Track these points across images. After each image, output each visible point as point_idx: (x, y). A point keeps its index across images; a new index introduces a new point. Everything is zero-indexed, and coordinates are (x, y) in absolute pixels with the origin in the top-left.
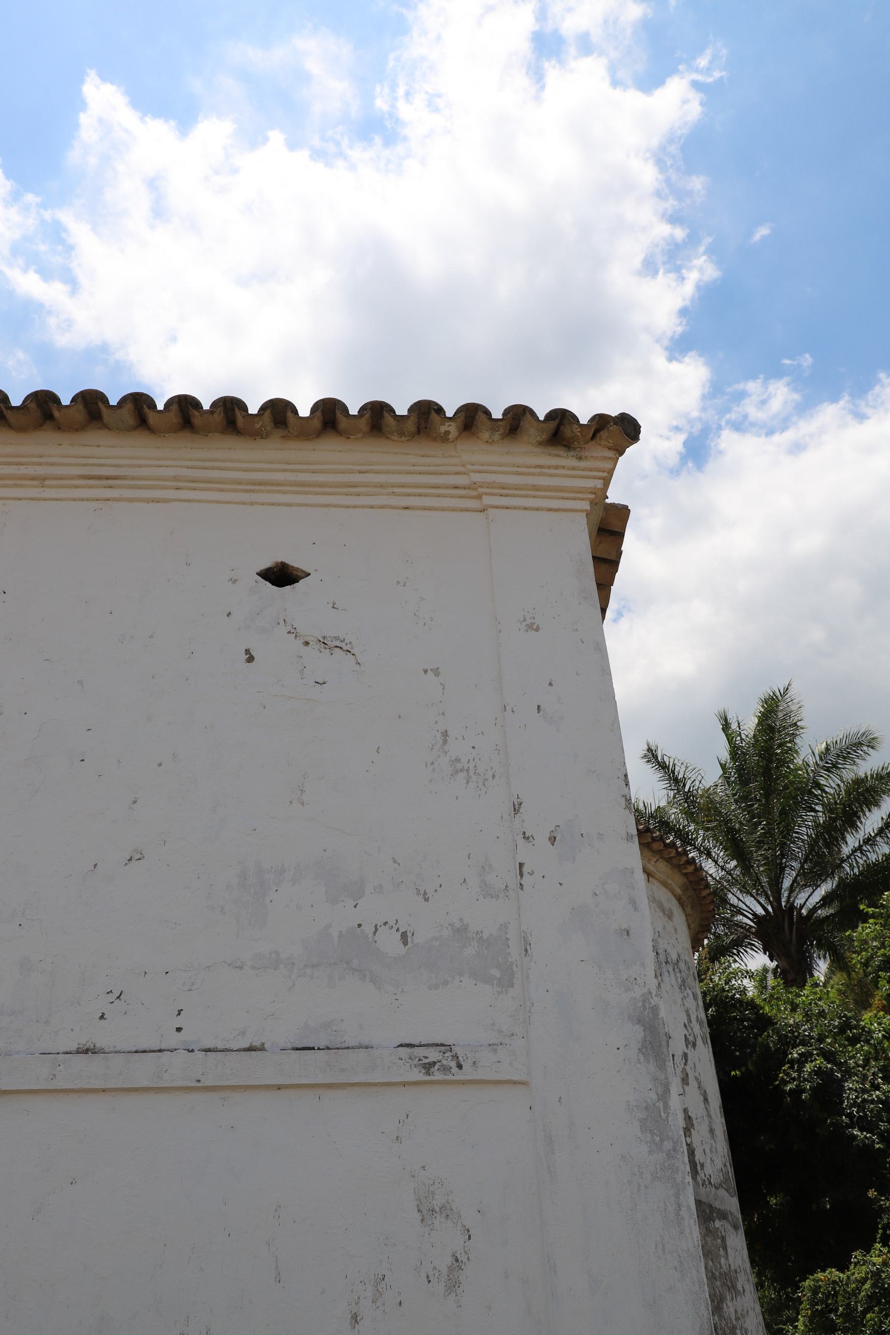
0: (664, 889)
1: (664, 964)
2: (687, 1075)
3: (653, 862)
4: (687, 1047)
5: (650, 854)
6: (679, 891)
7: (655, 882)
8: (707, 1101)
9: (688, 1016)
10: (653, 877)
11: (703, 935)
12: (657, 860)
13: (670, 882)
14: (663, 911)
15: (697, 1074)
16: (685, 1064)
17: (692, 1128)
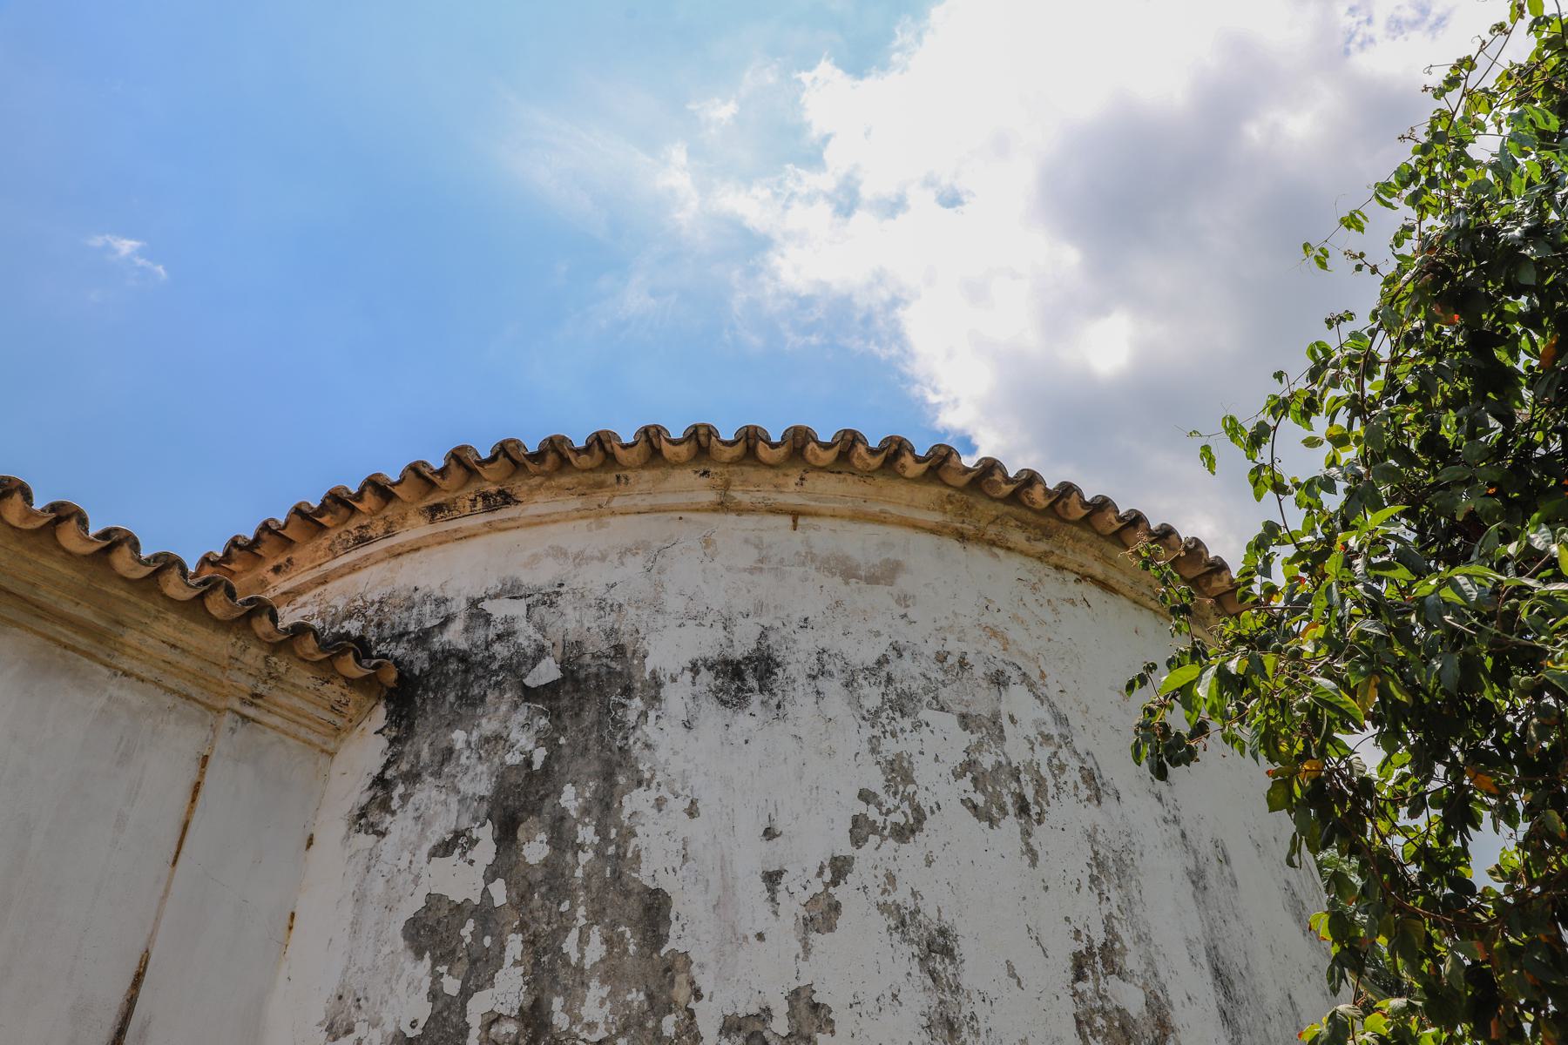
0: (870, 528)
1: (802, 680)
2: (836, 908)
3: (792, 487)
4: (857, 841)
5: (769, 474)
6: (935, 518)
7: (826, 523)
8: (947, 952)
9: (899, 772)
10: (816, 514)
11: (1220, 580)
12: (802, 479)
13: (875, 508)
14: (848, 572)
15: (901, 896)
16: (835, 883)
17: (820, 1029)
